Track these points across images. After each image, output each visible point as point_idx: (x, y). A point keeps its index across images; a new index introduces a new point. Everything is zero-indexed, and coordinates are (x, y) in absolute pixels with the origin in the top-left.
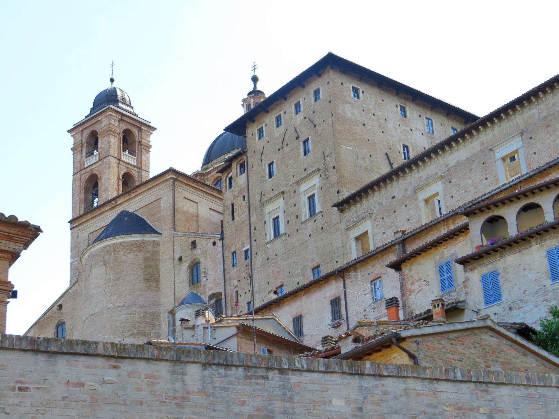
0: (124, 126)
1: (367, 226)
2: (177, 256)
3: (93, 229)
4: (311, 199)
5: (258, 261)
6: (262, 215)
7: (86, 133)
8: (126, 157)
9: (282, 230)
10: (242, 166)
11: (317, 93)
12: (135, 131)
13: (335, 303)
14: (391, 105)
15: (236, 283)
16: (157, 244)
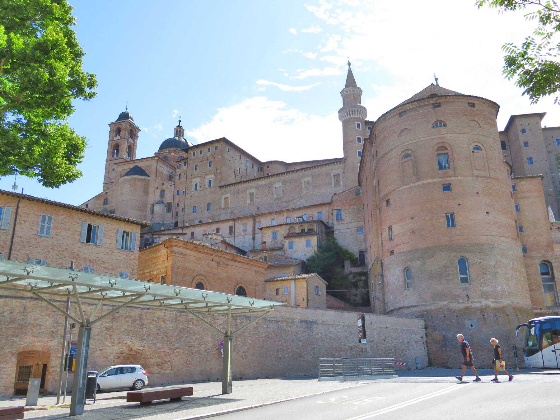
0: (131, 128)
1: (228, 195)
2: (156, 186)
3: (123, 168)
4: (210, 182)
5: (188, 196)
6: (191, 182)
7: (116, 127)
8: (131, 140)
9: (198, 188)
10: (185, 163)
11: (216, 147)
12: (134, 130)
13: (231, 228)
14: (238, 154)
15: (178, 200)
16: (149, 180)
